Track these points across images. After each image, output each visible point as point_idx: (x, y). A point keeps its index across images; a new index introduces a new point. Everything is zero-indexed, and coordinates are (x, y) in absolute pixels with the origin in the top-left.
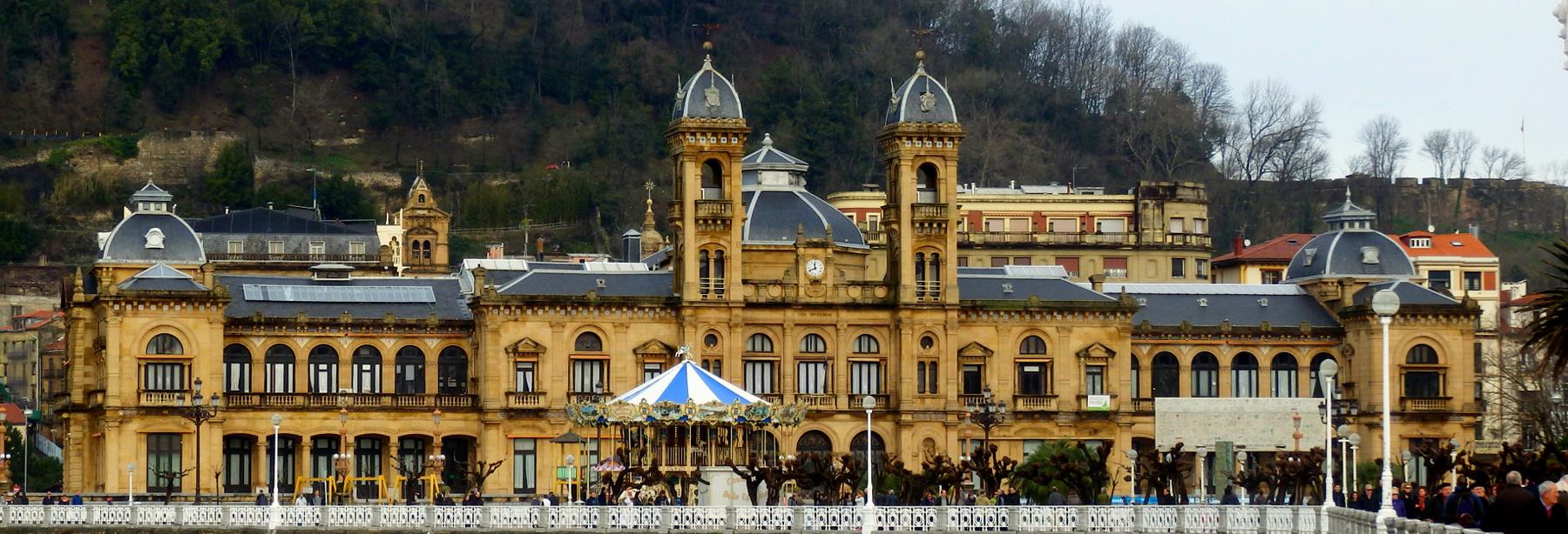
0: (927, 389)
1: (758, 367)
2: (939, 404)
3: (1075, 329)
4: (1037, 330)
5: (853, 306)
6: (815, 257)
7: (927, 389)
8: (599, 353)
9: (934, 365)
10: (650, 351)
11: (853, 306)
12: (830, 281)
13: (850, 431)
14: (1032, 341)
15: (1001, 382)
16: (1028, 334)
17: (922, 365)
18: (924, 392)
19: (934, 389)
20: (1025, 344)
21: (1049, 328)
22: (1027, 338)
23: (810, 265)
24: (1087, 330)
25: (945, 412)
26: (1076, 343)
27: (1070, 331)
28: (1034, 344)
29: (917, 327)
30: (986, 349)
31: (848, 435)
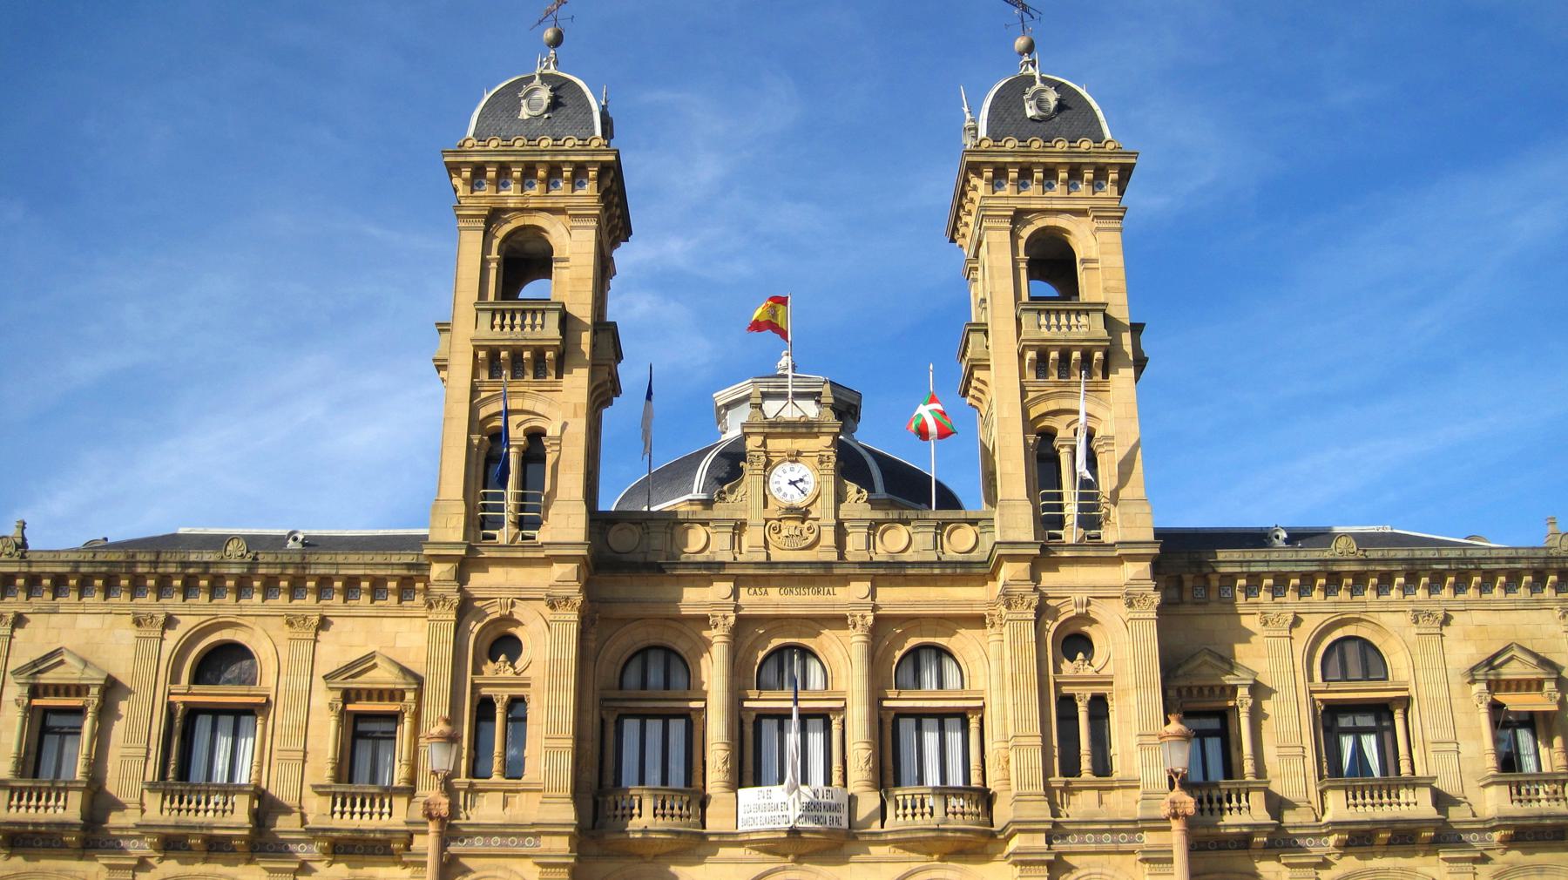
0: (1085, 764)
1: (655, 727)
2: (1121, 804)
3: (1457, 618)
5: (894, 572)
6: (796, 457)
7: (1085, 764)
8: (243, 689)
9: (1099, 706)
10: (362, 682)
11: (894, 572)
16: (1338, 634)
17: (1067, 704)
18: (1078, 773)
19: (1102, 766)
20: (1336, 656)
23: (782, 476)
25: (1138, 826)
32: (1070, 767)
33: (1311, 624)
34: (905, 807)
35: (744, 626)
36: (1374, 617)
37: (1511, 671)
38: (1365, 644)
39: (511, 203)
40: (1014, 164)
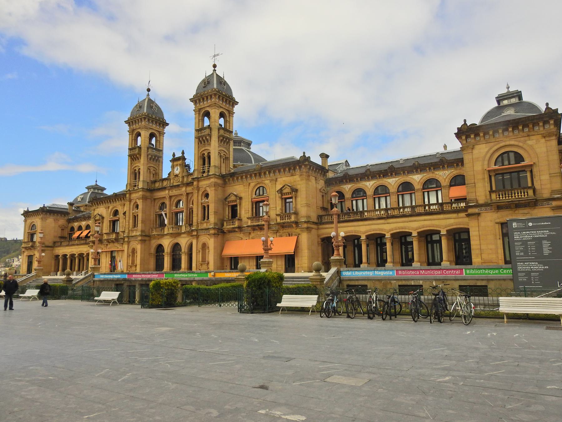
3: (278, 179)
4: (262, 183)
6: (177, 165)
12: (180, 175)
13: (188, 241)
14: (261, 188)
15: (245, 211)
16: (258, 186)
21: (267, 182)
22: (259, 188)
24: (284, 179)
26: (279, 187)
27: (276, 180)
28: (260, 189)
29: (201, 189)
30: (236, 196)
31: (186, 243)
32: (204, 219)
33: (252, 185)
34: (177, 229)
35: (171, 197)
36: (263, 182)
37: (284, 191)
38: (263, 187)
39: (135, 128)
40: (197, 99)
